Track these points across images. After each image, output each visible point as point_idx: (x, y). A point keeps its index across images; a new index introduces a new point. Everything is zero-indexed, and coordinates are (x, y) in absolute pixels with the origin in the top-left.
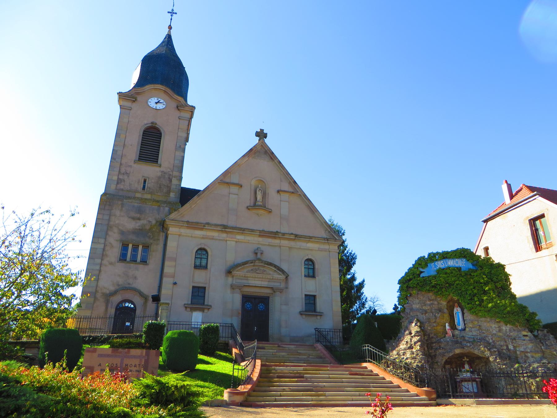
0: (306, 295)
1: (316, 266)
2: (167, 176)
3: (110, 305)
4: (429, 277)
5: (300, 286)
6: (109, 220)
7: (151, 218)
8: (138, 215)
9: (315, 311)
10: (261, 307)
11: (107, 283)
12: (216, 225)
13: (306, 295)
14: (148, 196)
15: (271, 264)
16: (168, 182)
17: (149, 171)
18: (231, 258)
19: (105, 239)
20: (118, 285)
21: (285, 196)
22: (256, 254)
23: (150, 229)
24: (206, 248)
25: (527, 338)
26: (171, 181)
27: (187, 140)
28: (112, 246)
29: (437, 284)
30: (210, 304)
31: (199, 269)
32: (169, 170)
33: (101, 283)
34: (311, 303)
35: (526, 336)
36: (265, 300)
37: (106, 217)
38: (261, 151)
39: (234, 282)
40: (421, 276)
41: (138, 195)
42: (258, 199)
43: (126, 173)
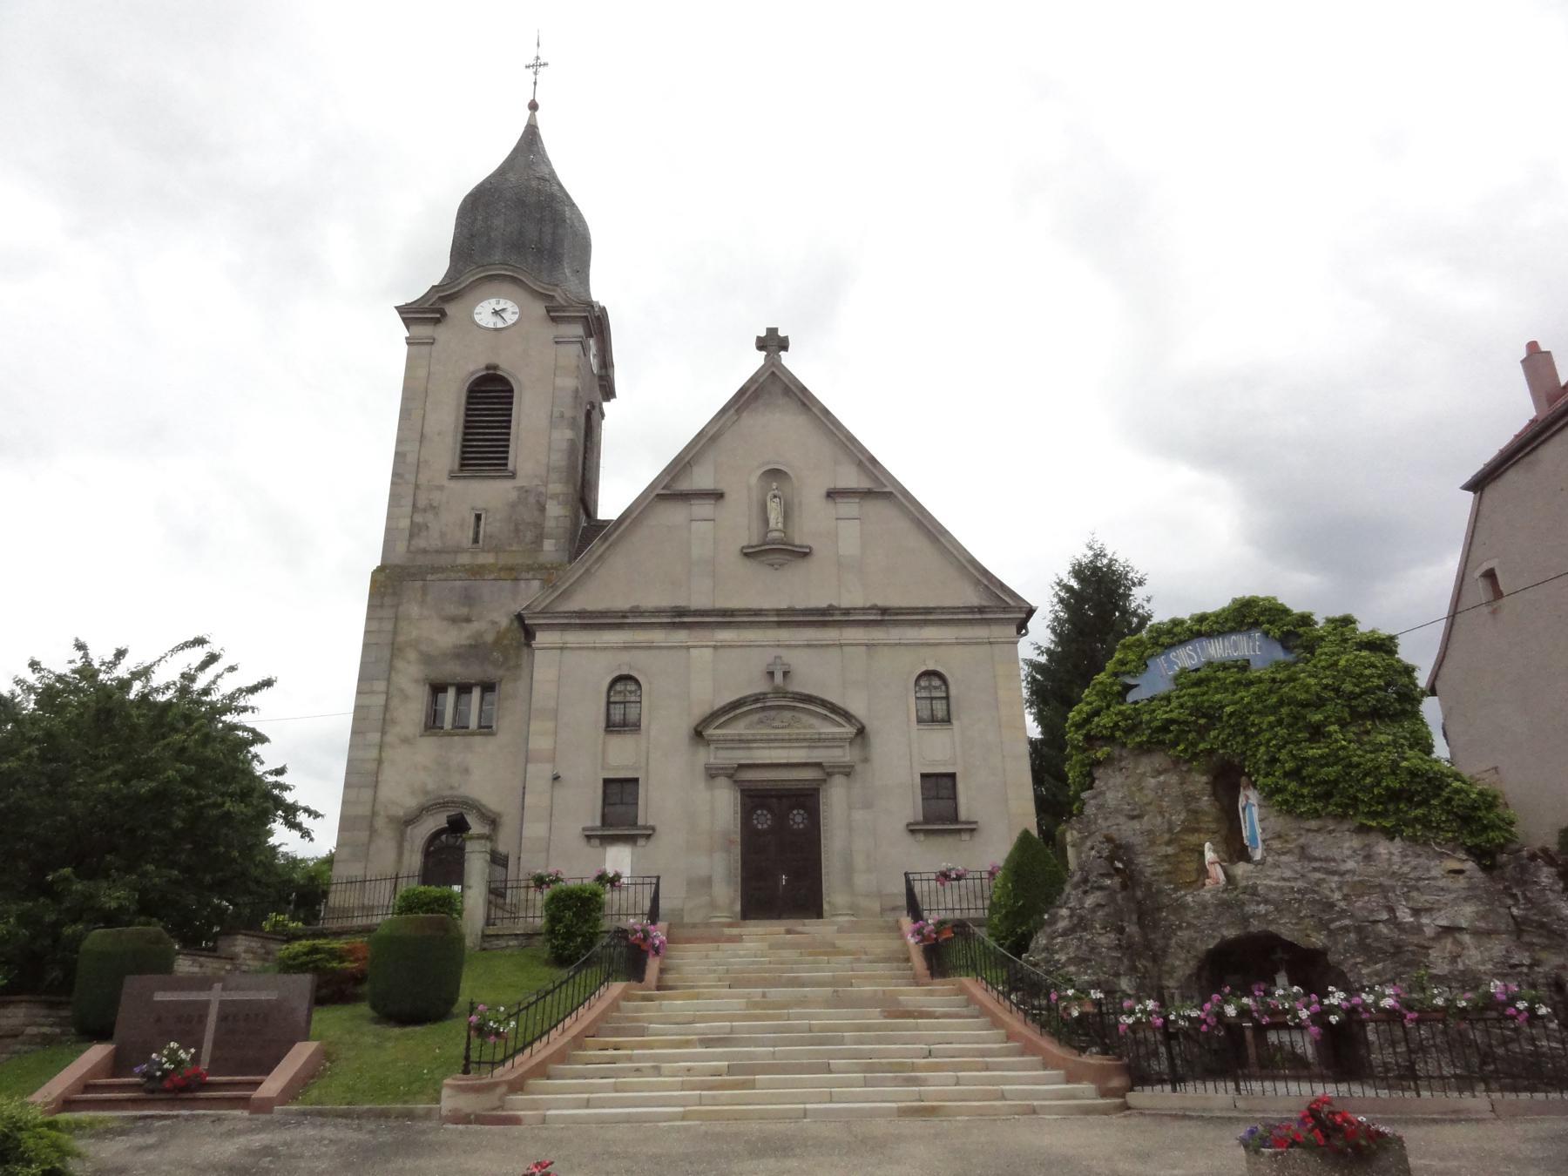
0: (923, 776)
1: (953, 691)
2: (532, 500)
3: (407, 845)
4: (1151, 699)
5: (903, 752)
6: (395, 632)
7: (497, 612)
8: (465, 611)
9: (955, 819)
10: (798, 819)
11: (399, 793)
12: (658, 612)
13: (923, 776)
14: (487, 559)
15: (809, 699)
16: (536, 513)
17: (489, 493)
18: (707, 693)
19: (389, 680)
20: (426, 793)
21: (849, 508)
22: (771, 674)
23: (497, 642)
24: (632, 673)
25: (1462, 882)
26: (542, 509)
27: (609, 393)
28: (406, 698)
29: (1173, 721)
30: (651, 823)
31: (619, 732)
32: (536, 482)
33: (385, 792)
34: (940, 803)
35: (1460, 872)
36: (806, 799)
37: (388, 626)
38: (772, 388)
39: (712, 760)
40: (1131, 697)
41: (464, 559)
42: (772, 524)
43: (433, 508)
